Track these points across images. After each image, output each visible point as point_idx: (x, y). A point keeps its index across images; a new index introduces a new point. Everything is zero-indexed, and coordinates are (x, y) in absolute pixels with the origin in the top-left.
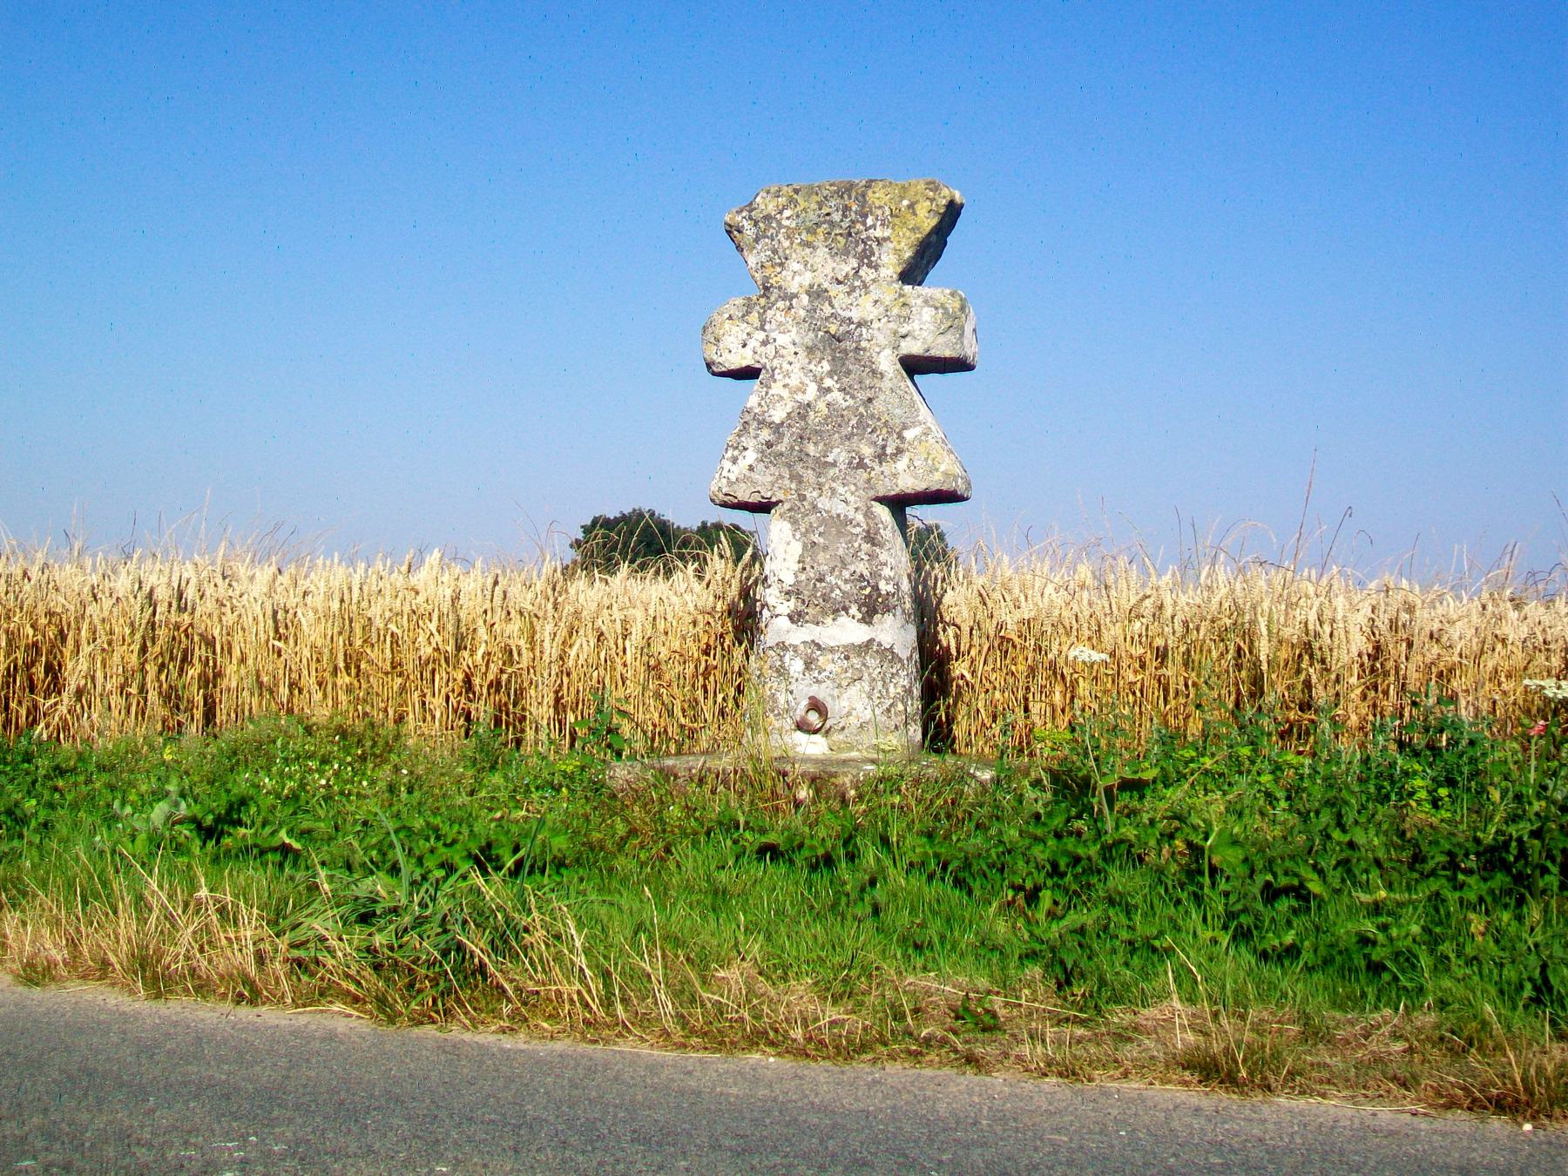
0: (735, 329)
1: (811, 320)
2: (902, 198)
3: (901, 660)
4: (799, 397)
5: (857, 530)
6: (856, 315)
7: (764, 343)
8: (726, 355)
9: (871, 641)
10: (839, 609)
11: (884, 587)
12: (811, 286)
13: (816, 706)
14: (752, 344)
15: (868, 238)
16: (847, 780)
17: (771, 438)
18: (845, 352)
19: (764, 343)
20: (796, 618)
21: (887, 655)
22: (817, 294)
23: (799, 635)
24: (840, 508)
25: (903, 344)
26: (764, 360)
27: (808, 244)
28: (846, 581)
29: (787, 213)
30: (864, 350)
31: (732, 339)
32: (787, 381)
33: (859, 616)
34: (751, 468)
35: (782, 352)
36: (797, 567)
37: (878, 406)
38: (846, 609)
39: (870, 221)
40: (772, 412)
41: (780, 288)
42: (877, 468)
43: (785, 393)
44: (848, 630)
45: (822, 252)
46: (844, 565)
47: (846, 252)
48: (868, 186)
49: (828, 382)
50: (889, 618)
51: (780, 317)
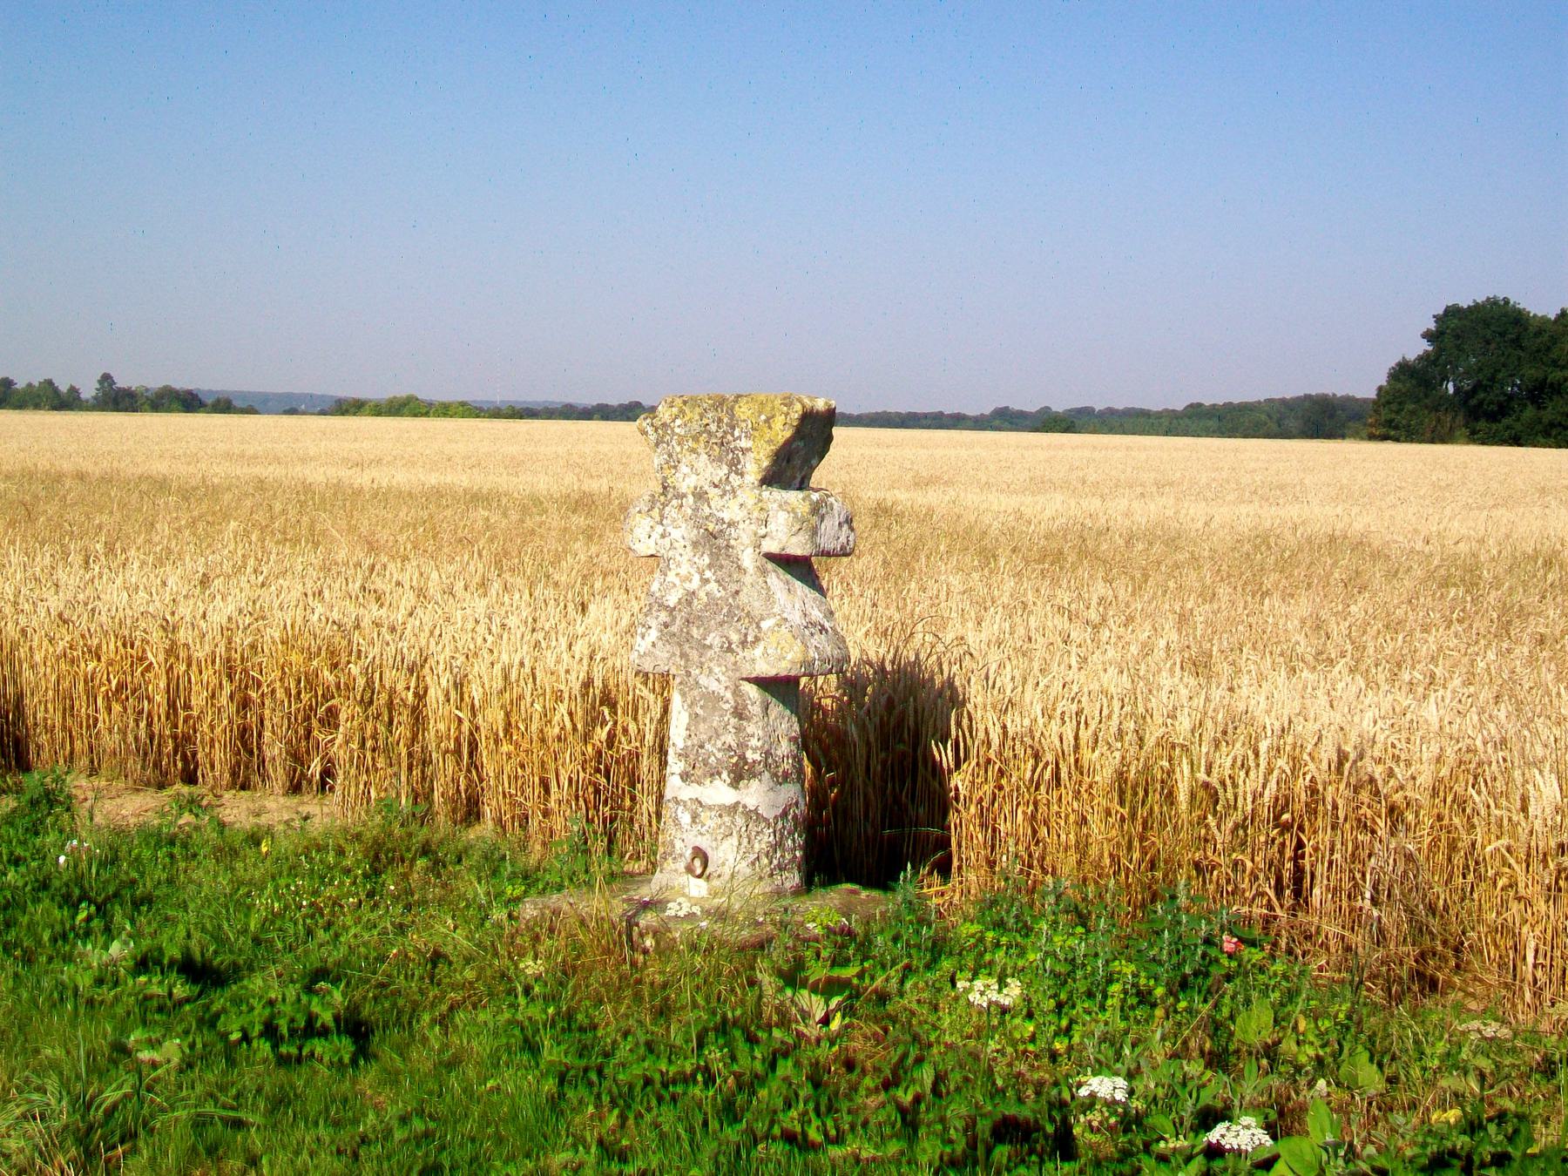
1: (696, 520)
2: (760, 413)
3: (766, 820)
4: (687, 585)
5: (726, 706)
6: (726, 516)
7: (663, 536)
10: (714, 774)
11: (750, 756)
13: (699, 853)
14: (655, 535)
17: (668, 619)
18: (719, 548)
19: (663, 536)
20: (685, 777)
21: (753, 815)
22: (700, 495)
23: (688, 792)
27: (693, 451)
29: (678, 422)
34: (654, 645)
37: (743, 598)
39: (737, 433)
43: (677, 581)
44: (719, 792)
46: (718, 736)
47: (720, 460)
48: (736, 401)
49: (708, 574)
50: (754, 783)
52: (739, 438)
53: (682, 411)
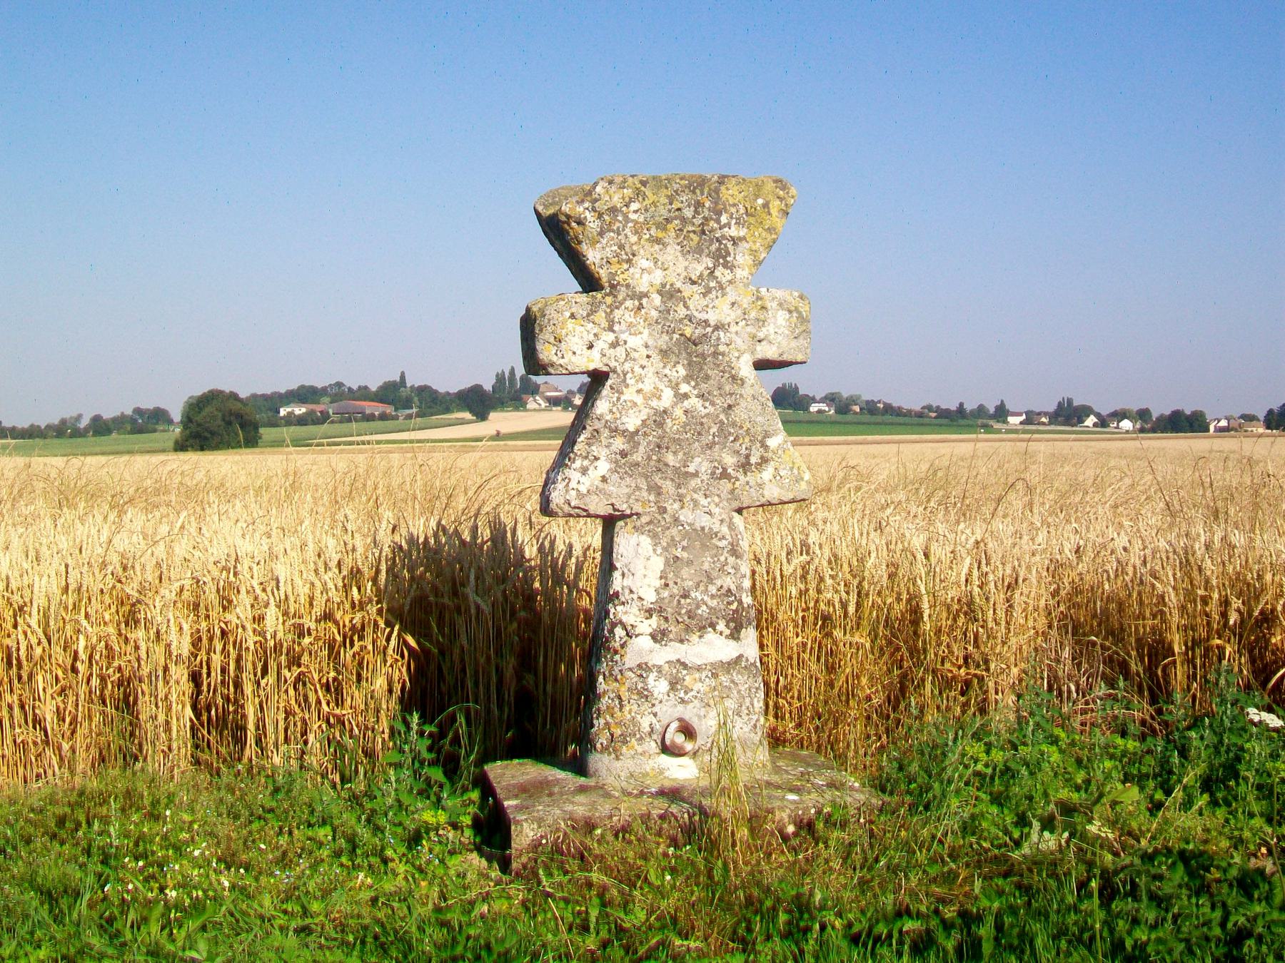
0: (579, 329)
1: (664, 322)
2: (757, 197)
4: (654, 403)
5: (723, 543)
6: (712, 317)
7: (614, 345)
8: (569, 356)
9: (741, 656)
12: (664, 285)
14: (600, 345)
15: (723, 237)
16: (785, 815)
17: (626, 447)
18: (703, 356)
19: (614, 345)
20: (659, 636)
22: (670, 294)
24: (705, 521)
25: (759, 348)
26: (613, 364)
27: (658, 241)
28: (713, 597)
29: (634, 206)
30: (723, 354)
31: (576, 339)
32: (640, 386)
33: (728, 632)
34: (604, 479)
35: (634, 355)
36: (658, 583)
37: (740, 414)
38: (713, 626)
39: (724, 219)
40: (624, 419)
41: (628, 286)
42: (742, 477)
43: (639, 399)
45: (673, 250)
46: (710, 580)
47: (699, 250)
49: (684, 388)
51: (629, 317)
52: (728, 225)
53: (638, 193)
